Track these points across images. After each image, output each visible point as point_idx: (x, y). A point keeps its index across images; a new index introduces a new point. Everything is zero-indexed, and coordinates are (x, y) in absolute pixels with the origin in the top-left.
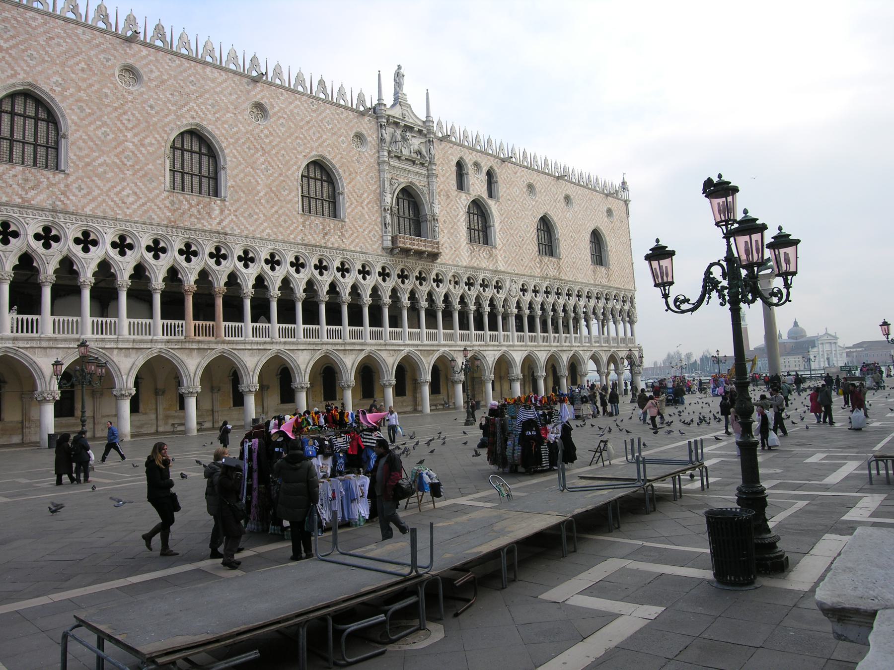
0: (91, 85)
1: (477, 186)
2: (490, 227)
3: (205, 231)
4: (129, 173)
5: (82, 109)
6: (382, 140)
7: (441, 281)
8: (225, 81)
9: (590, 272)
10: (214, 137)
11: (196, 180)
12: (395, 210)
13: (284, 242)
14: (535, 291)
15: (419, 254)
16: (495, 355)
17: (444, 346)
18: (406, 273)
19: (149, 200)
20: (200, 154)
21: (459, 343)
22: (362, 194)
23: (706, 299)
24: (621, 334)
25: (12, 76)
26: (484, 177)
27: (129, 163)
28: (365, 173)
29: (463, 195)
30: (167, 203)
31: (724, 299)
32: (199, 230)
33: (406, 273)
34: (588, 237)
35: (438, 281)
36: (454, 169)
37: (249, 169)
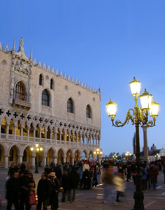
1: (47, 84)
2: (50, 100)
6: (13, 63)
7: (30, 118)
9: (85, 120)
12: (15, 89)
14: (65, 125)
15: (23, 107)
16: (48, 148)
17: (29, 143)
18: (17, 114)
22: (3, 82)
23: (127, 122)
24: (95, 144)
28: (5, 75)
31: (134, 123)
33: (17, 114)
34: (85, 107)
35: (29, 118)
36: (39, 77)
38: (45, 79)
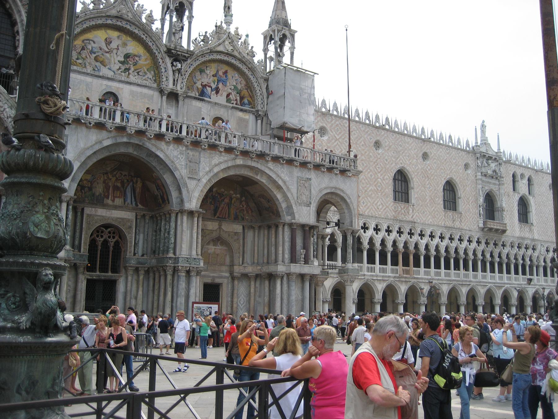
0: (366, 152)
2: (529, 212)
3: (407, 221)
4: (380, 194)
5: (363, 164)
8: (413, 143)
10: (409, 173)
11: (400, 194)
13: (438, 226)
15: (497, 230)
17: (507, 284)
19: (387, 207)
20: (402, 181)
21: (514, 282)
25: (341, 151)
26: (525, 181)
27: (379, 189)
29: (516, 195)
30: (393, 208)
32: (405, 221)
35: (503, 245)
36: (512, 179)
37: (423, 188)
38: (520, 180)
